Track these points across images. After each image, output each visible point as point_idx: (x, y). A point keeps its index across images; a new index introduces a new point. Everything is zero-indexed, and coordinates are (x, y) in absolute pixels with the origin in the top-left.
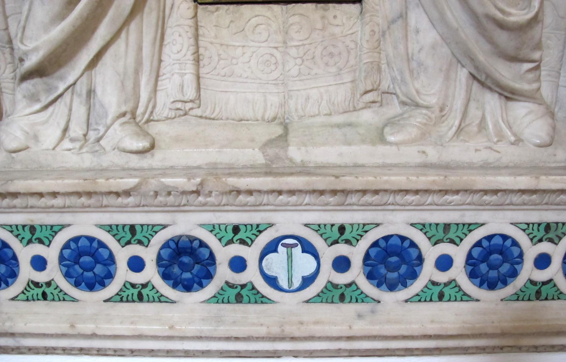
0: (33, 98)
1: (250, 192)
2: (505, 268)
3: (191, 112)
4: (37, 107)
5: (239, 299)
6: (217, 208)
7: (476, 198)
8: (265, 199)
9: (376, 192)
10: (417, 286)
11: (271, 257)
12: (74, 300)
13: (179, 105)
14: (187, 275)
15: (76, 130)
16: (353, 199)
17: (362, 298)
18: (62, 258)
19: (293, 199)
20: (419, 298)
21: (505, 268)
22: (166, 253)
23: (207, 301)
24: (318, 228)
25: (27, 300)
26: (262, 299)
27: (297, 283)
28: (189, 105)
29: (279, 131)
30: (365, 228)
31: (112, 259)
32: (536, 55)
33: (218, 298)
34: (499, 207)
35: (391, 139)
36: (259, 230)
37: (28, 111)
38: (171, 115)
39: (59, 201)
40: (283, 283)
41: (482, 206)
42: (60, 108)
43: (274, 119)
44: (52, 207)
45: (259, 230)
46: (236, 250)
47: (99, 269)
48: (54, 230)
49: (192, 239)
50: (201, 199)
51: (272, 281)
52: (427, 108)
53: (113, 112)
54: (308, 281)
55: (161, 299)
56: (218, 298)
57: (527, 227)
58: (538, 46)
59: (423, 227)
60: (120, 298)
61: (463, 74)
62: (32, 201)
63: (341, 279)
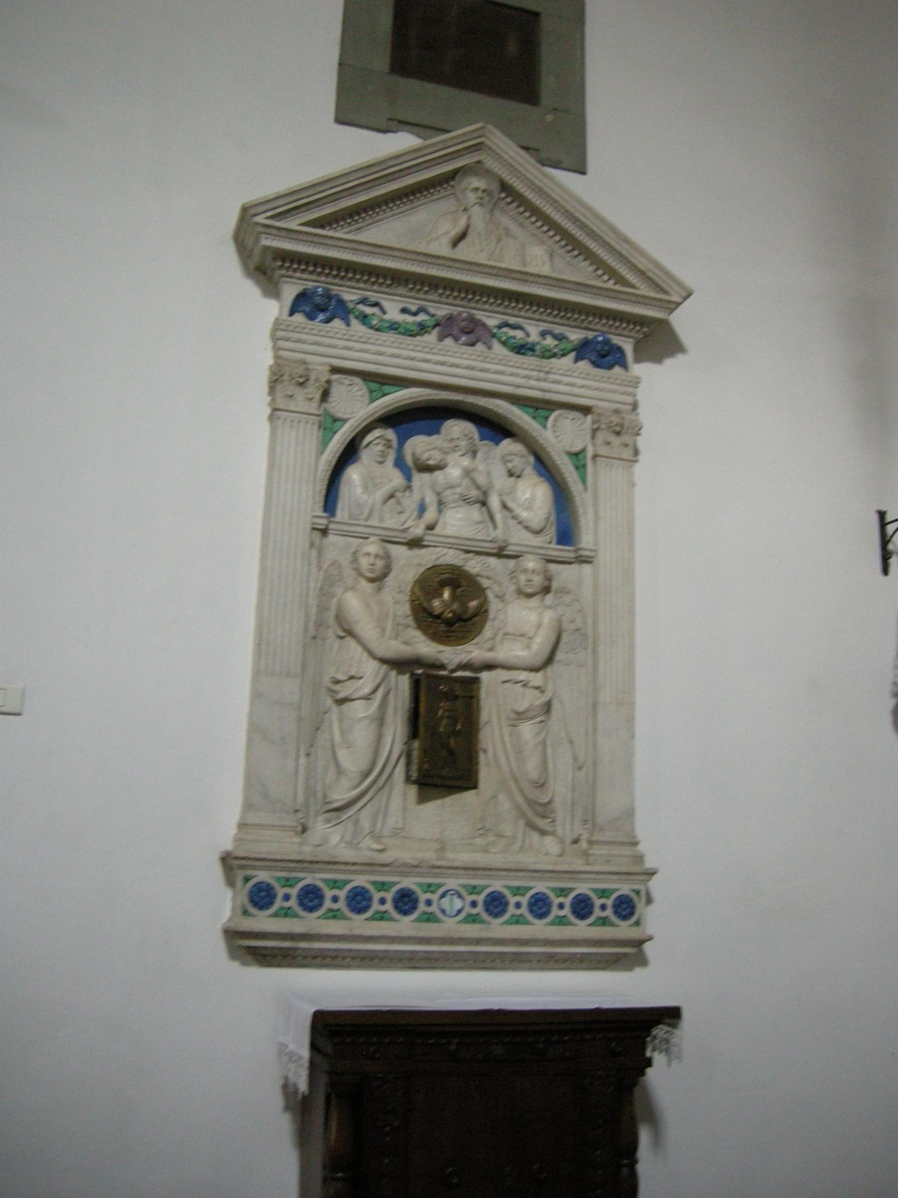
0: (328, 821)
1: (439, 867)
2: (544, 909)
3: (402, 834)
4: (329, 825)
5: (428, 920)
6: (422, 875)
7: (528, 874)
8: (446, 871)
9: (490, 869)
10: (506, 917)
11: (443, 899)
12: (350, 919)
13: (395, 830)
14: (406, 907)
15: (348, 838)
16: (480, 872)
17: (482, 922)
18: (348, 897)
19: (456, 872)
20: (508, 922)
21: (544, 909)
22: (398, 896)
23: (415, 921)
24: (464, 886)
25: (324, 918)
26: (438, 921)
27: (454, 913)
28: (399, 831)
29: (439, 846)
30: (485, 887)
31: (370, 899)
32: (552, 815)
33: (418, 920)
34: (540, 879)
35: (492, 850)
36: (439, 886)
37: (324, 827)
38: (391, 835)
39: (354, 868)
40: (448, 912)
41: (533, 879)
42: (340, 827)
43: (436, 840)
44: (349, 870)
45: (439, 886)
46: (428, 896)
47: (364, 903)
48: (346, 882)
49: (410, 890)
50: (418, 870)
51: (443, 911)
52: (506, 837)
53: (367, 831)
54: (459, 912)
55: (392, 919)
56: (418, 920)
57: (553, 889)
58: (553, 812)
59: (509, 888)
60: (372, 918)
61: (522, 823)
62: (342, 867)
63: (475, 911)
